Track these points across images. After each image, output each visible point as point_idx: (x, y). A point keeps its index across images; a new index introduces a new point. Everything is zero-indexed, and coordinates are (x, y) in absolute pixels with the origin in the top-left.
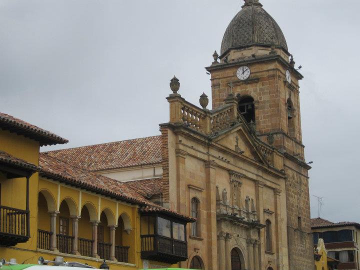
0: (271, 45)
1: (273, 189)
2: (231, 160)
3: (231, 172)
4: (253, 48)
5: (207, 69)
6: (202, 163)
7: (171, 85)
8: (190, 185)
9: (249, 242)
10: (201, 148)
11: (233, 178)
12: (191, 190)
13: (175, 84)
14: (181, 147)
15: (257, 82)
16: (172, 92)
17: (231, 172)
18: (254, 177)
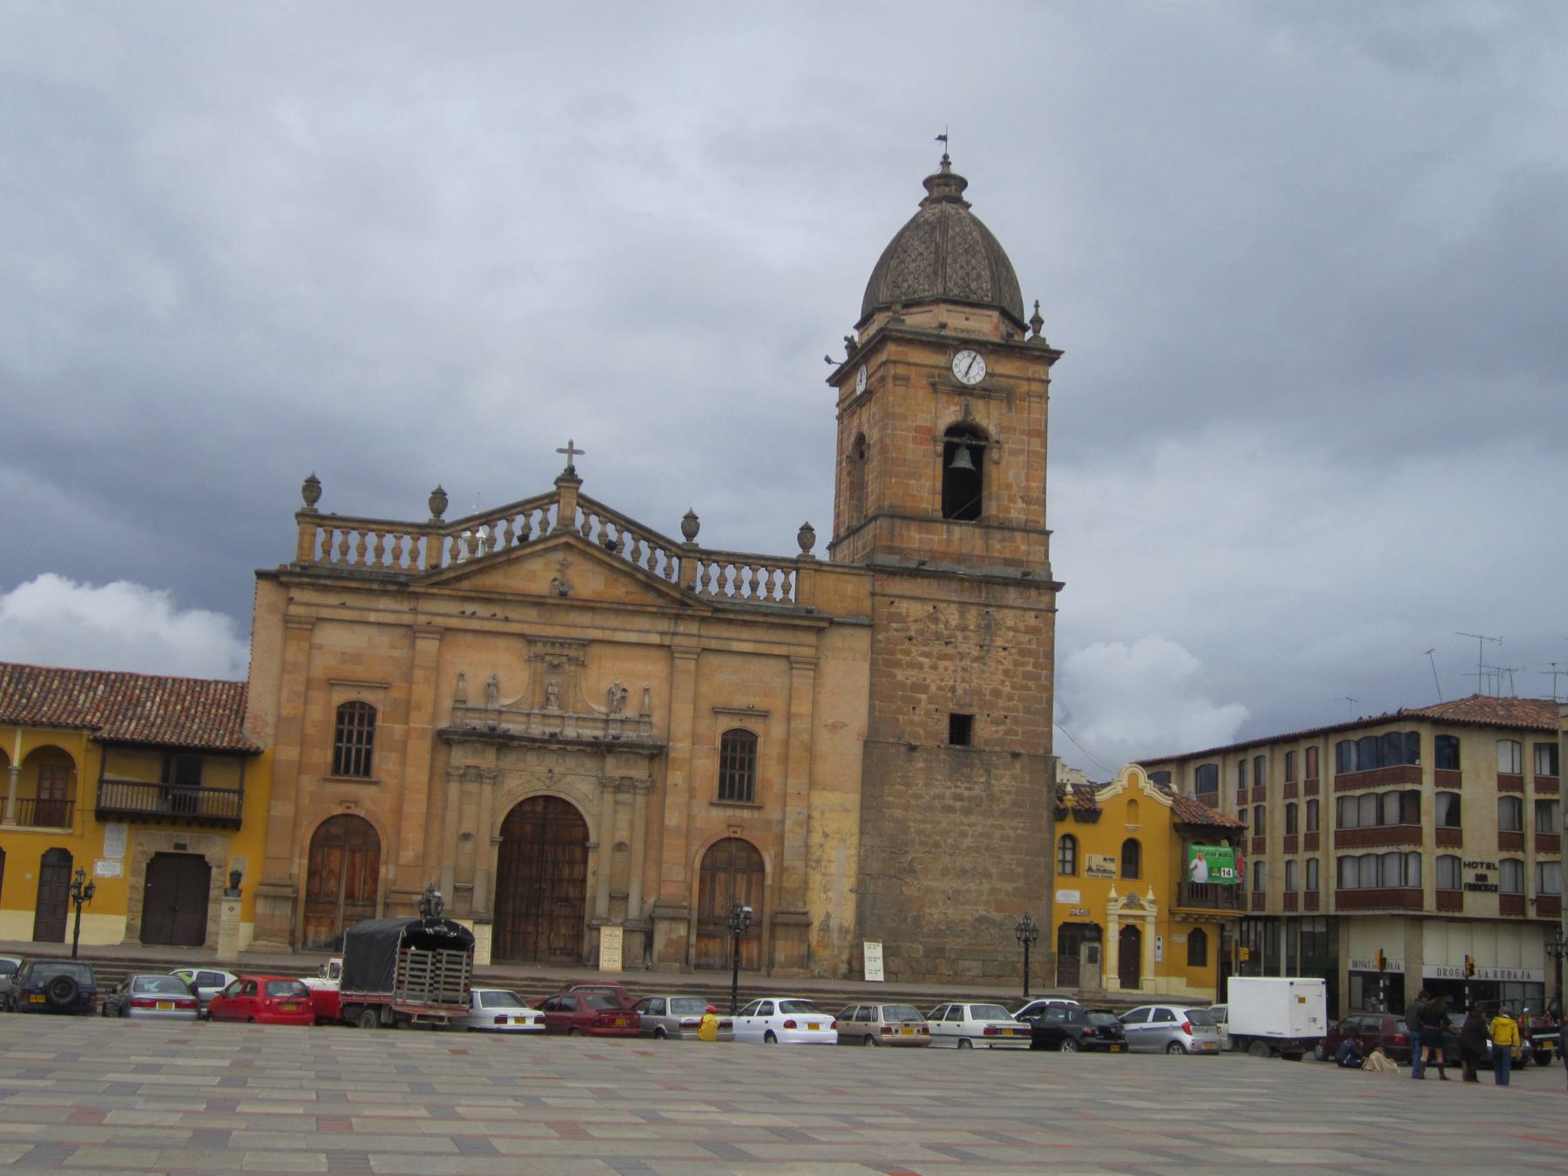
0: (891, 303)
1: (787, 657)
2: (532, 613)
3: (529, 640)
4: (875, 317)
5: (829, 381)
6: (402, 631)
7: (305, 489)
8: (329, 680)
9: (603, 784)
10: (385, 603)
11: (540, 648)
12: (336, 689)
13: (312, 488)
14: (293, 610)
15: (870, 400)
16: (304, 504)
17: (529, 640)
18: (655, 639)
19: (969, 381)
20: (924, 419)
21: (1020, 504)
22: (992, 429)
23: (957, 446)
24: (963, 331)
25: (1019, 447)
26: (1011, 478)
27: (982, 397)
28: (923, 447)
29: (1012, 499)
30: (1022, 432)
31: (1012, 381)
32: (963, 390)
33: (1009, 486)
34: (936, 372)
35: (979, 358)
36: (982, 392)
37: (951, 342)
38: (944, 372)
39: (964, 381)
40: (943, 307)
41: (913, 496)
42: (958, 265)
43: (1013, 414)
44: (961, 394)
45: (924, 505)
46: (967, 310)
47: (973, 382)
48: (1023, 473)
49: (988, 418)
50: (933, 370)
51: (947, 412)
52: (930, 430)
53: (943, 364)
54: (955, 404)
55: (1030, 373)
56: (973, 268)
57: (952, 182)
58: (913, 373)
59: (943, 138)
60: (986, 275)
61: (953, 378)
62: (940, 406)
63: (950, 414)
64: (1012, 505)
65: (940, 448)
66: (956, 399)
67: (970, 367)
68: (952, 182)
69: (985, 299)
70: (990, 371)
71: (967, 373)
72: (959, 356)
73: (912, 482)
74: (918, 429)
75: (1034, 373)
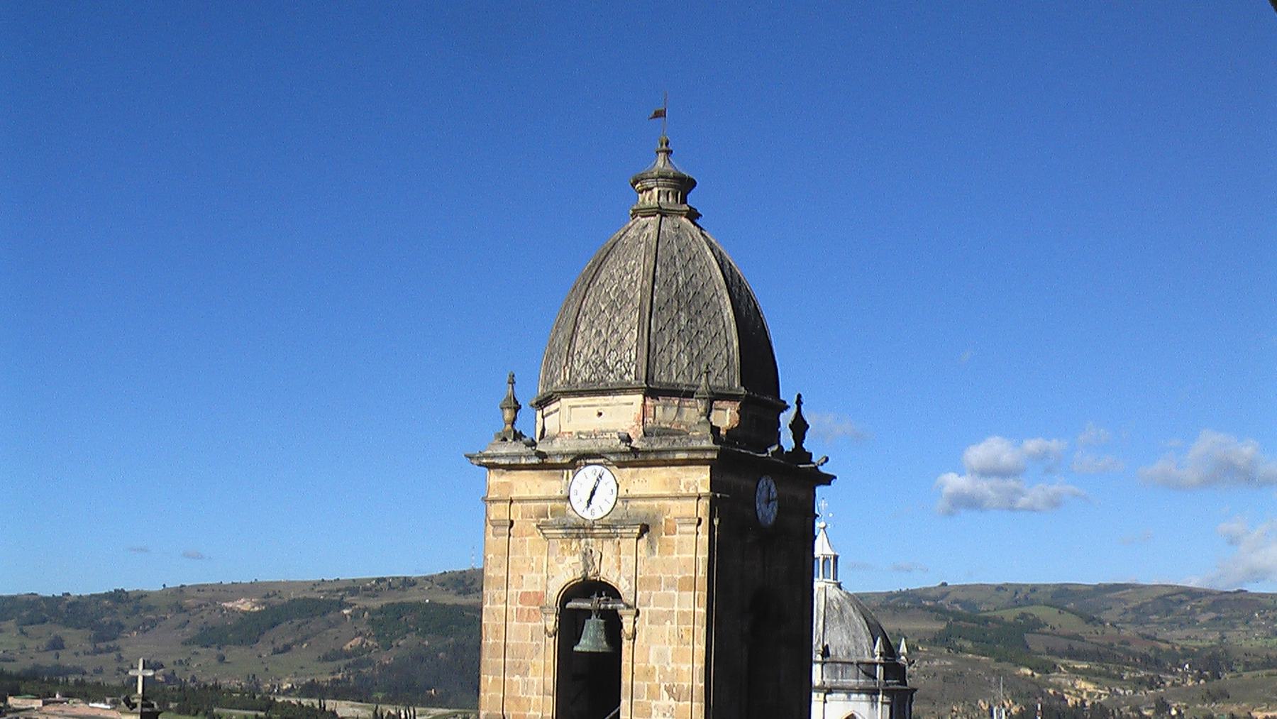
19: (592, 514)
20: (531, 582)
21: (666, 701)
22: (624, 587)
23: (587, 613)
24: (589, 435)
25: (665, 610)
26: (652, 663)
27: (610, 537)
28: (530, 624)
29: (654, 695)
30: (670, 585)
31: (655, 503)
32: (581, 530)
33: (649, 673)
34: (550, 504)
35: (607, 476)
36: (610, 528)
37: (559, 460)
38: (558, 504)
39: (587, 515)
40: (566, 402)
41: (518, 700)
42: (594, 331)
43: (657, 556)
44: (578, 537)
45: (532, 712)
46: (599, 400)
47: (598, 515)
48: (670, 650)
49: (619, 568)
50: (544, 504)
51: (561, 566)
52: (539, 598)
53: (558, 494)
54: (573, 553)
55: (682, 487)
56: (615, 331)
57: (649, 184)
58: (517, 511)
59: (659, 114)
60: (631, 339)
61: (571, 512)
62: (553, 558)
63: (567, 571)
64: (654, 703)
65: (551, 622)
66: (575, 544)
67: (593, 493)
68: (649, 184)
69: (627, 377)
70: (622, 492)
71: (589, 502)
72: (580, 475)
73: (517, 678)
74: (524, 597)
75: (688, 485)
